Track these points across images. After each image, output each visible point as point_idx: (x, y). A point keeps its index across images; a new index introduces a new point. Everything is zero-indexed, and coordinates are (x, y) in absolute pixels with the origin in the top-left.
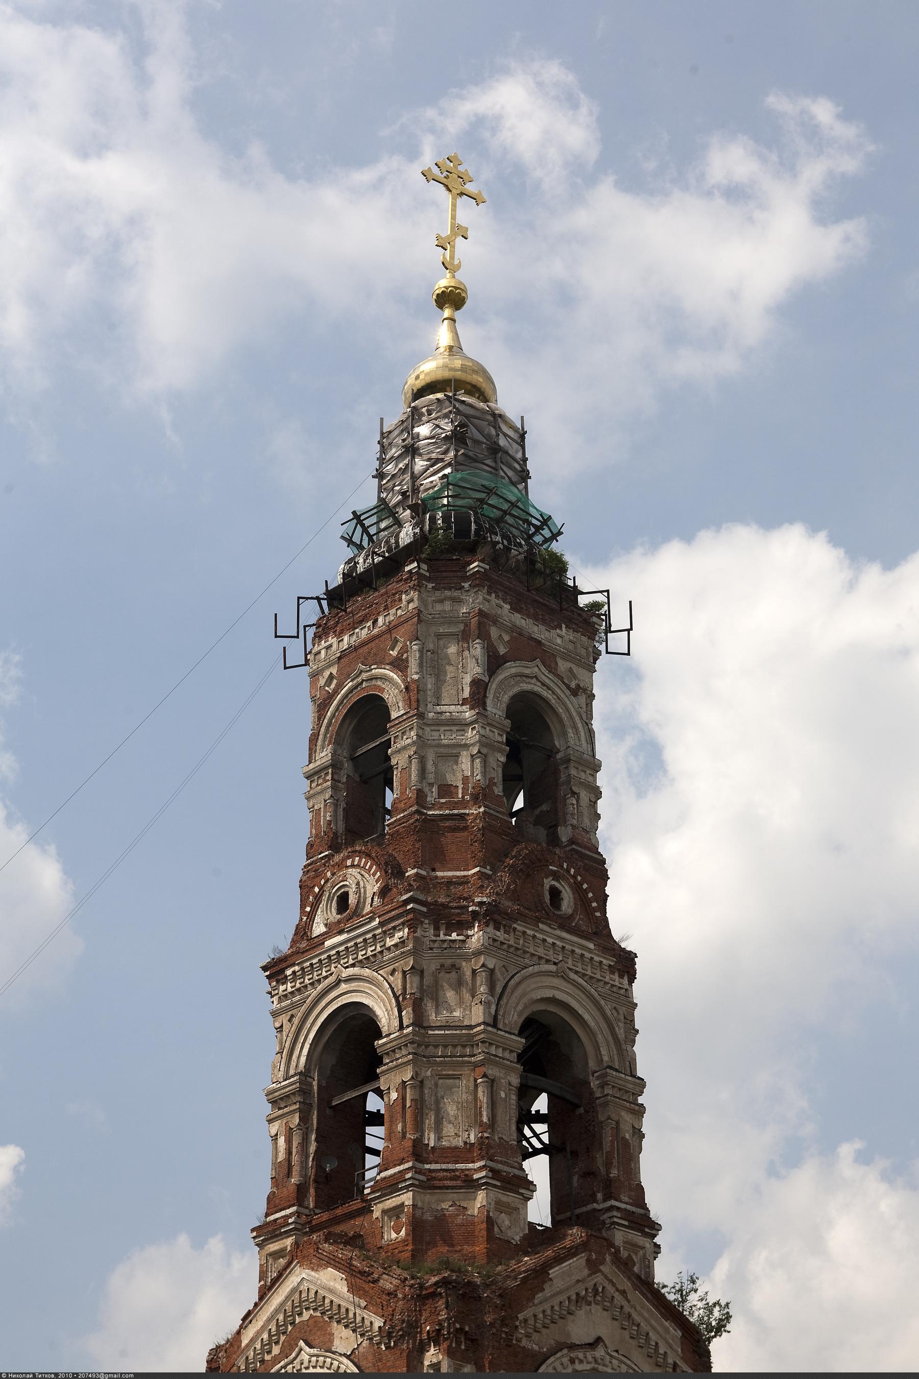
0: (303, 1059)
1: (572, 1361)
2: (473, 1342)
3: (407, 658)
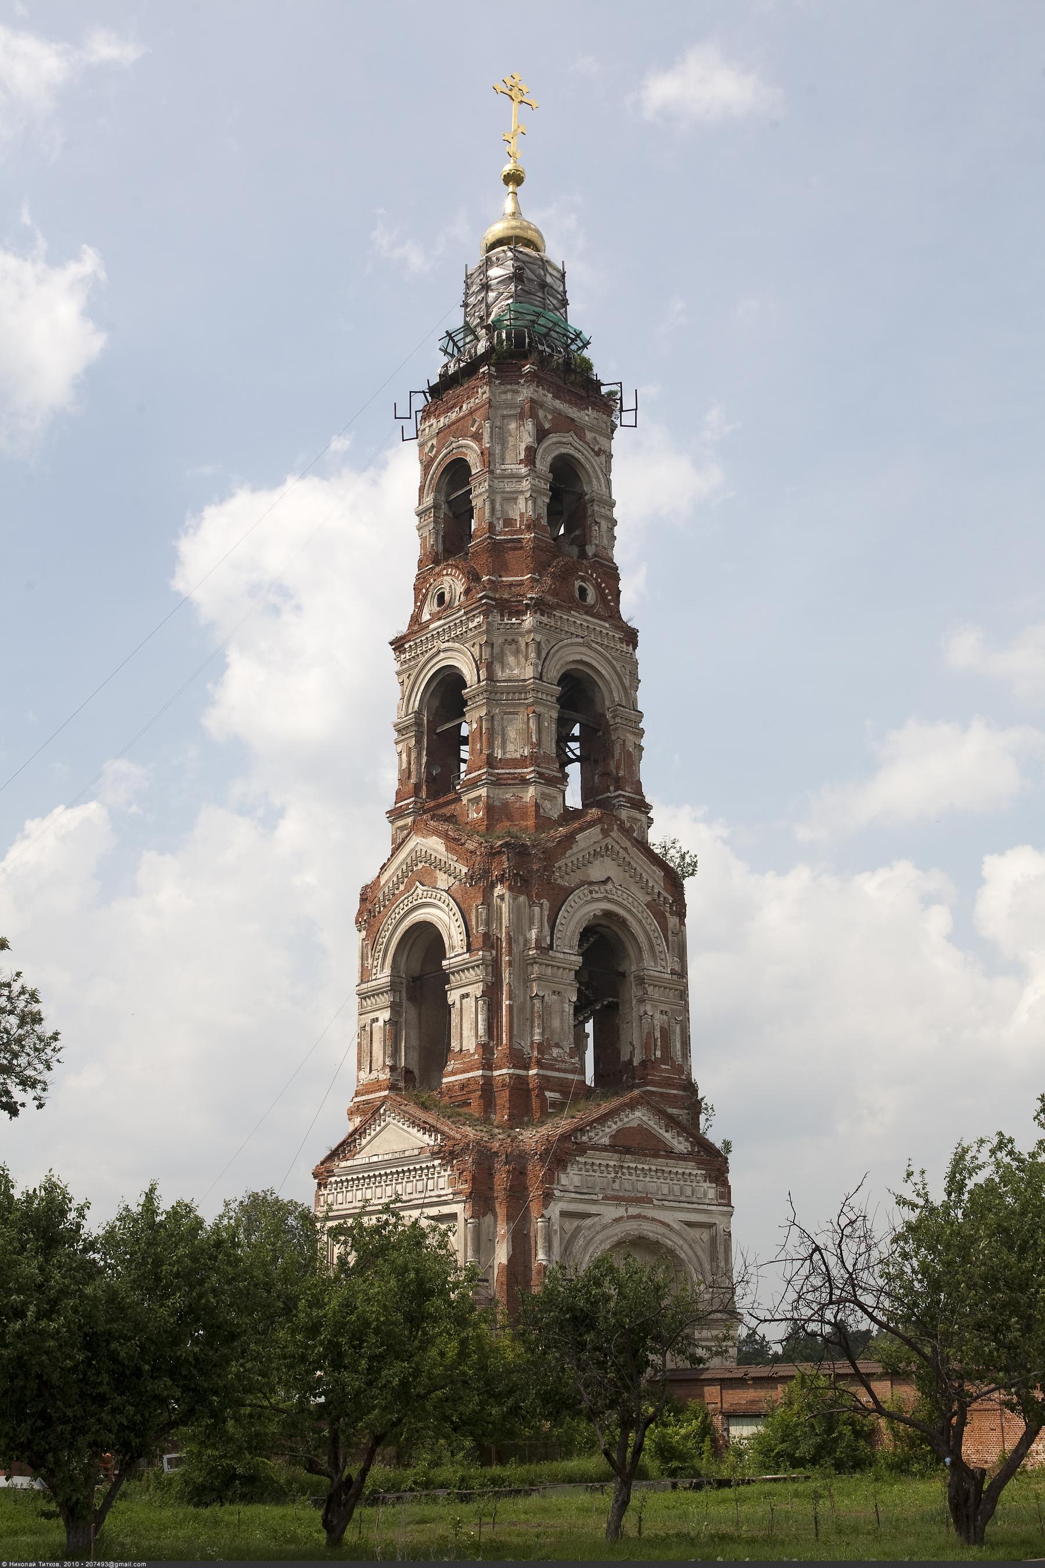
0: (417, 703)
1: (591, 892)
2: (526, 881)
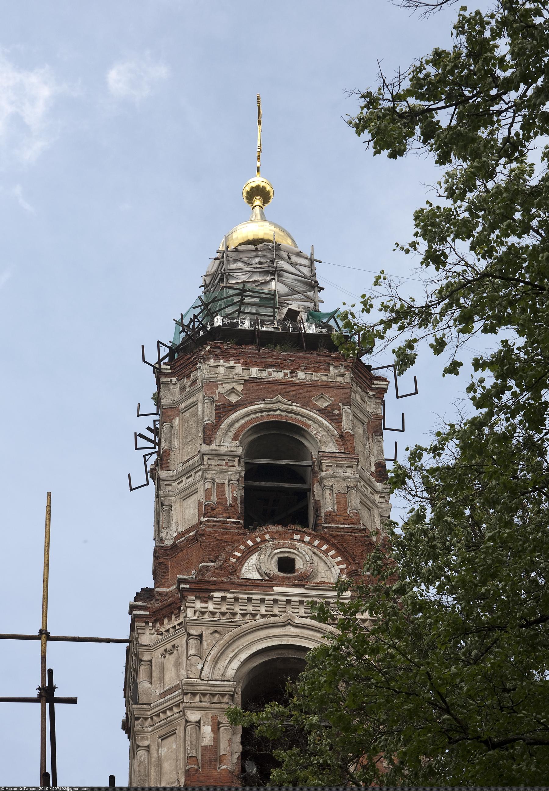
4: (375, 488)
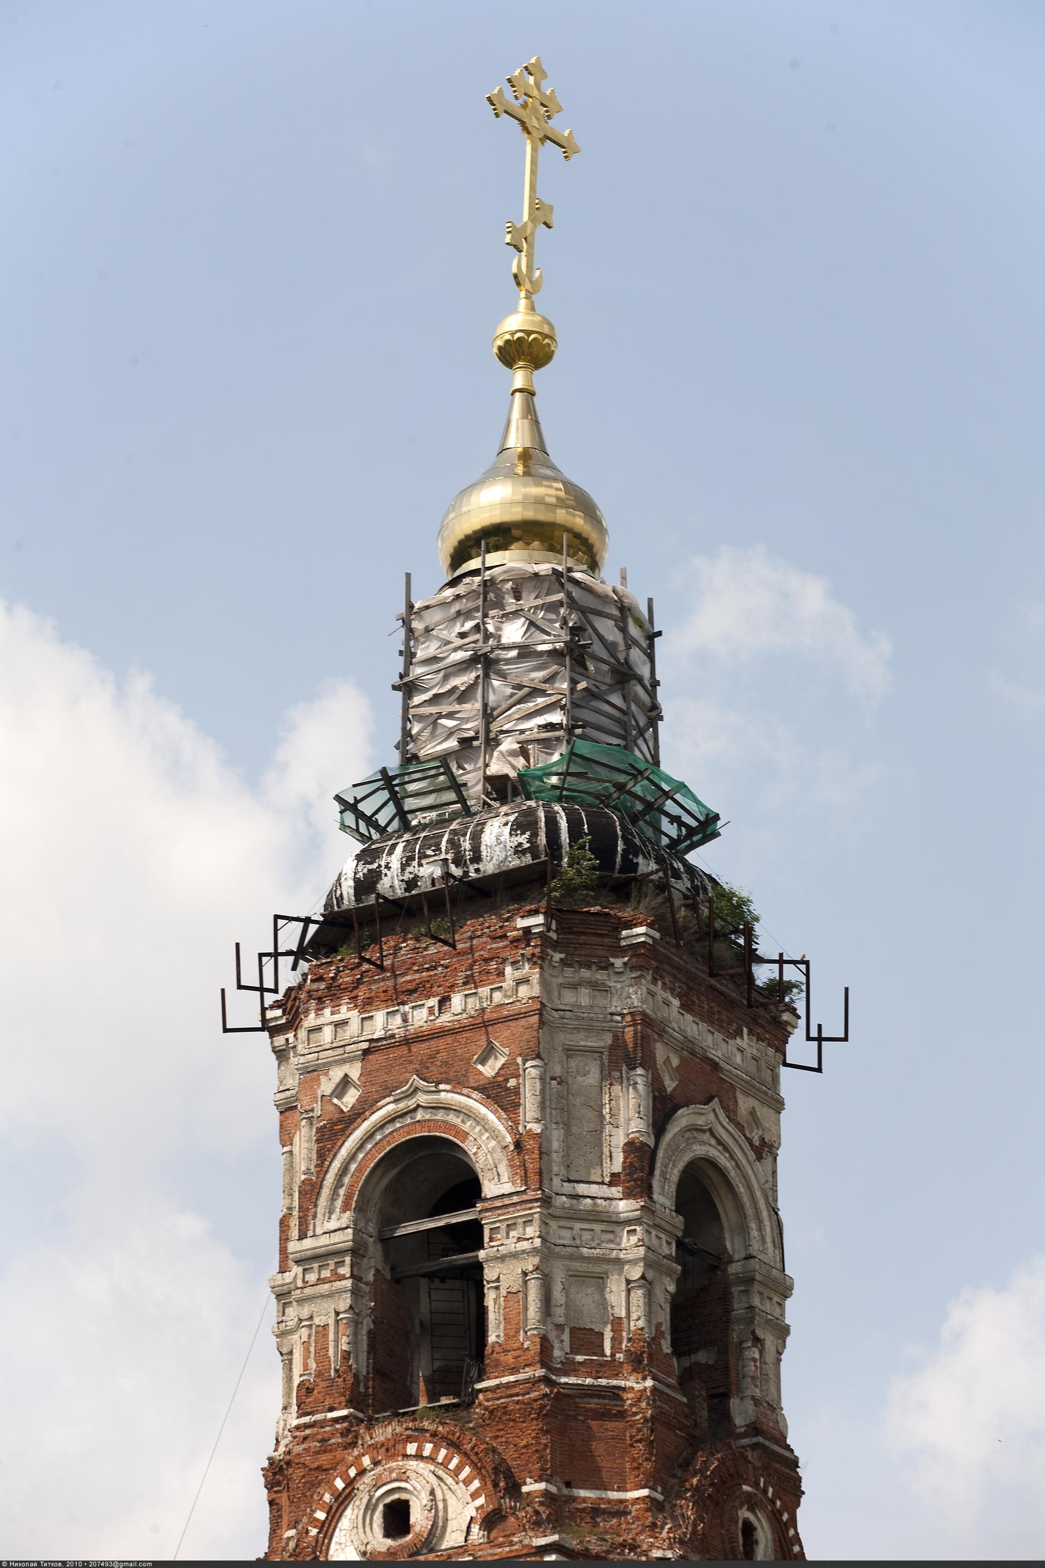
3: (517, 1088)
4: (614, 1219)
